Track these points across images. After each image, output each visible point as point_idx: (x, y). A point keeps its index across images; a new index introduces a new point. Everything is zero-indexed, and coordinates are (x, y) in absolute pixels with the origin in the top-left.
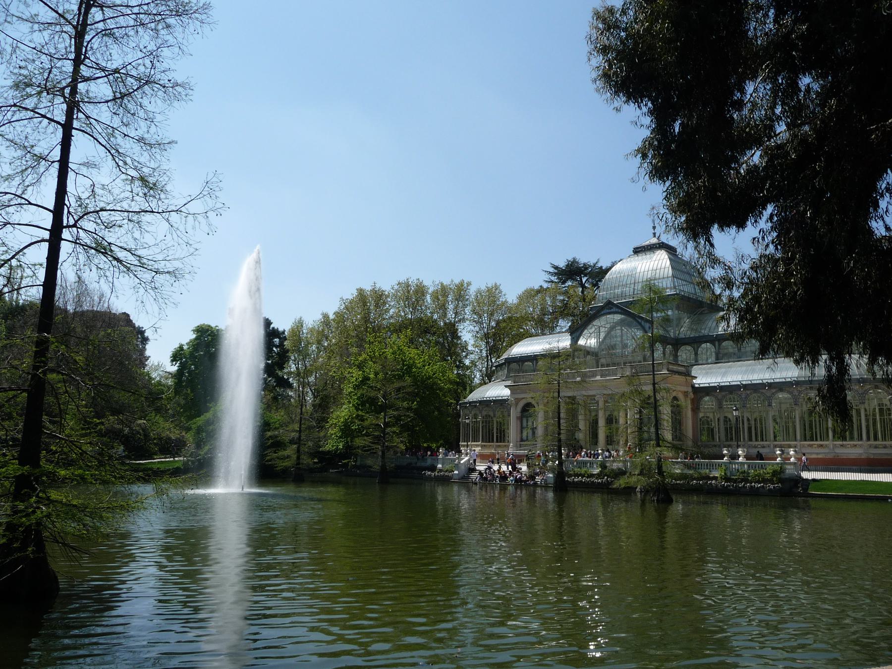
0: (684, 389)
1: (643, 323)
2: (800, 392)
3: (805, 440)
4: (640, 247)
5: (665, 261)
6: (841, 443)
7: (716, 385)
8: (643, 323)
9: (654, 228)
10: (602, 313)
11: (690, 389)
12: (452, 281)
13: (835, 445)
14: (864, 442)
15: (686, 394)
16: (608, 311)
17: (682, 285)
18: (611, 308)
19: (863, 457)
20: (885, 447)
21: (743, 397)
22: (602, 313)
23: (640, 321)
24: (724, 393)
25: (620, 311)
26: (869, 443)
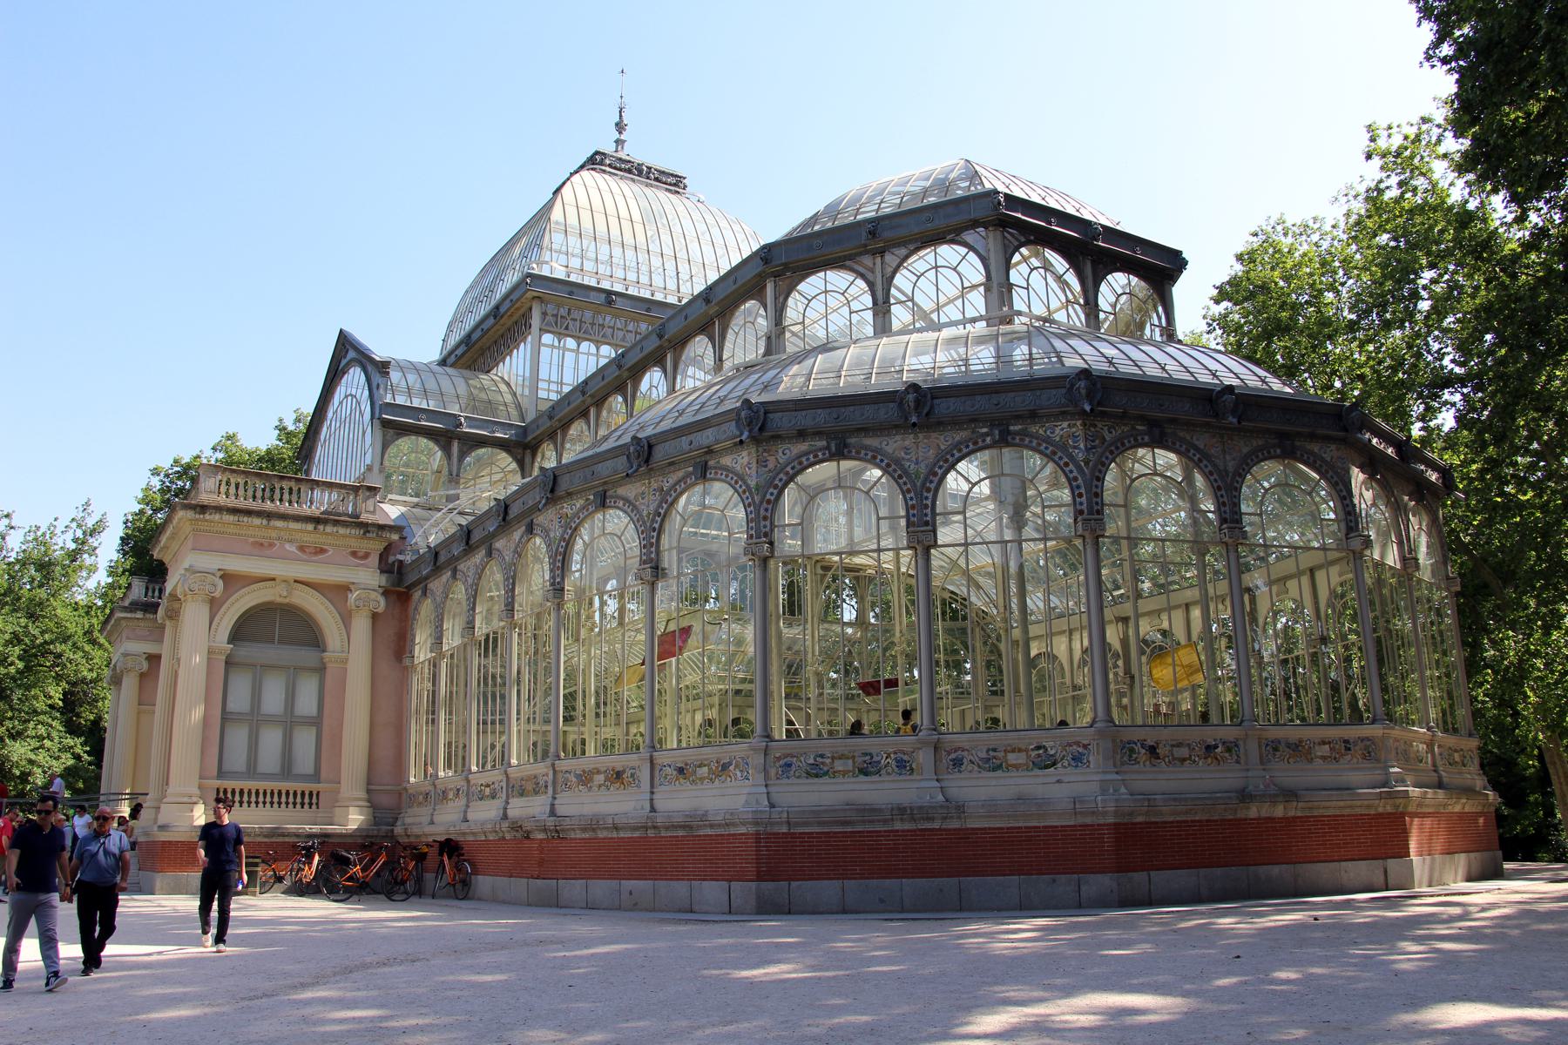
9: (620, 127)
19: (743, 830)
23: (370, 368)
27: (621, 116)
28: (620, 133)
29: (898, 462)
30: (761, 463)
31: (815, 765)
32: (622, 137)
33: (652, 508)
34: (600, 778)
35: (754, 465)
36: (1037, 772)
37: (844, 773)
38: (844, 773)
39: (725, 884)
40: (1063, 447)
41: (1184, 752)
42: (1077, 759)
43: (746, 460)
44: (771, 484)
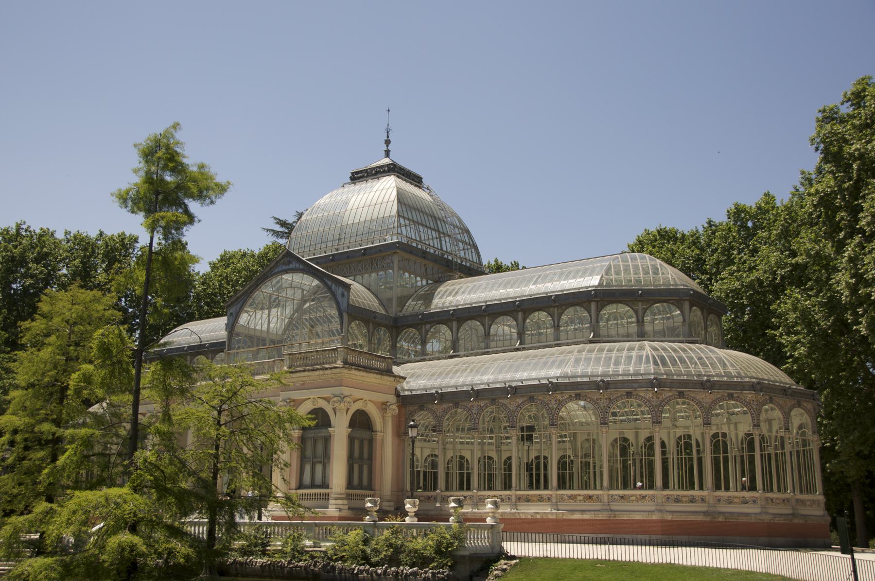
0: (382, 398)
1: (333, 286)
2: (561, 404)
3: (564, 488)
4: (361, 172)
5: (390, 190)
6: (621, 492)
7: (433, 391)
8: (333, 286)
9: (388, 142)
10: (277, 270)
11: (392, 399)
12: (101, 234)
13: (612, 496)
14: (659, 493)
15: (383, 407)
16: (284, 267)
17: (433, 239)
18: (290, 263)
20: (692, 500)
21: (474, 412)
22: (277, 270)
23: (329, 283)
24: (445, 406)
25: (301, 267)
26: (666, 492)
27: (388, 137)
28: (387, 146)
29: (700, 402)
30: (658, 398)
31: (677, 499)
32: (390, 148)
33: (605, 405)
34: (581, 498)
35: (655, 398)
36: (743, 505)
37: (686, 502)
38: (686, 502)
39: (648, 536)
40: (750, 403)
41: (778, 501)
42: (754, 502)
43: (651, 396)
44: (660, 405)
